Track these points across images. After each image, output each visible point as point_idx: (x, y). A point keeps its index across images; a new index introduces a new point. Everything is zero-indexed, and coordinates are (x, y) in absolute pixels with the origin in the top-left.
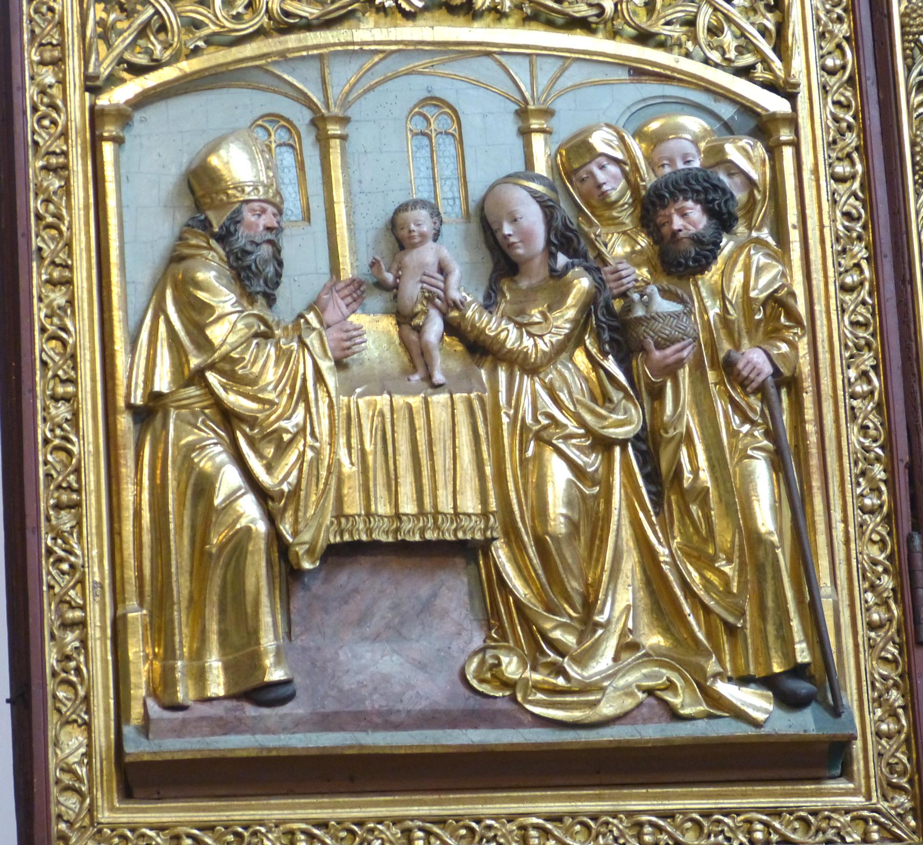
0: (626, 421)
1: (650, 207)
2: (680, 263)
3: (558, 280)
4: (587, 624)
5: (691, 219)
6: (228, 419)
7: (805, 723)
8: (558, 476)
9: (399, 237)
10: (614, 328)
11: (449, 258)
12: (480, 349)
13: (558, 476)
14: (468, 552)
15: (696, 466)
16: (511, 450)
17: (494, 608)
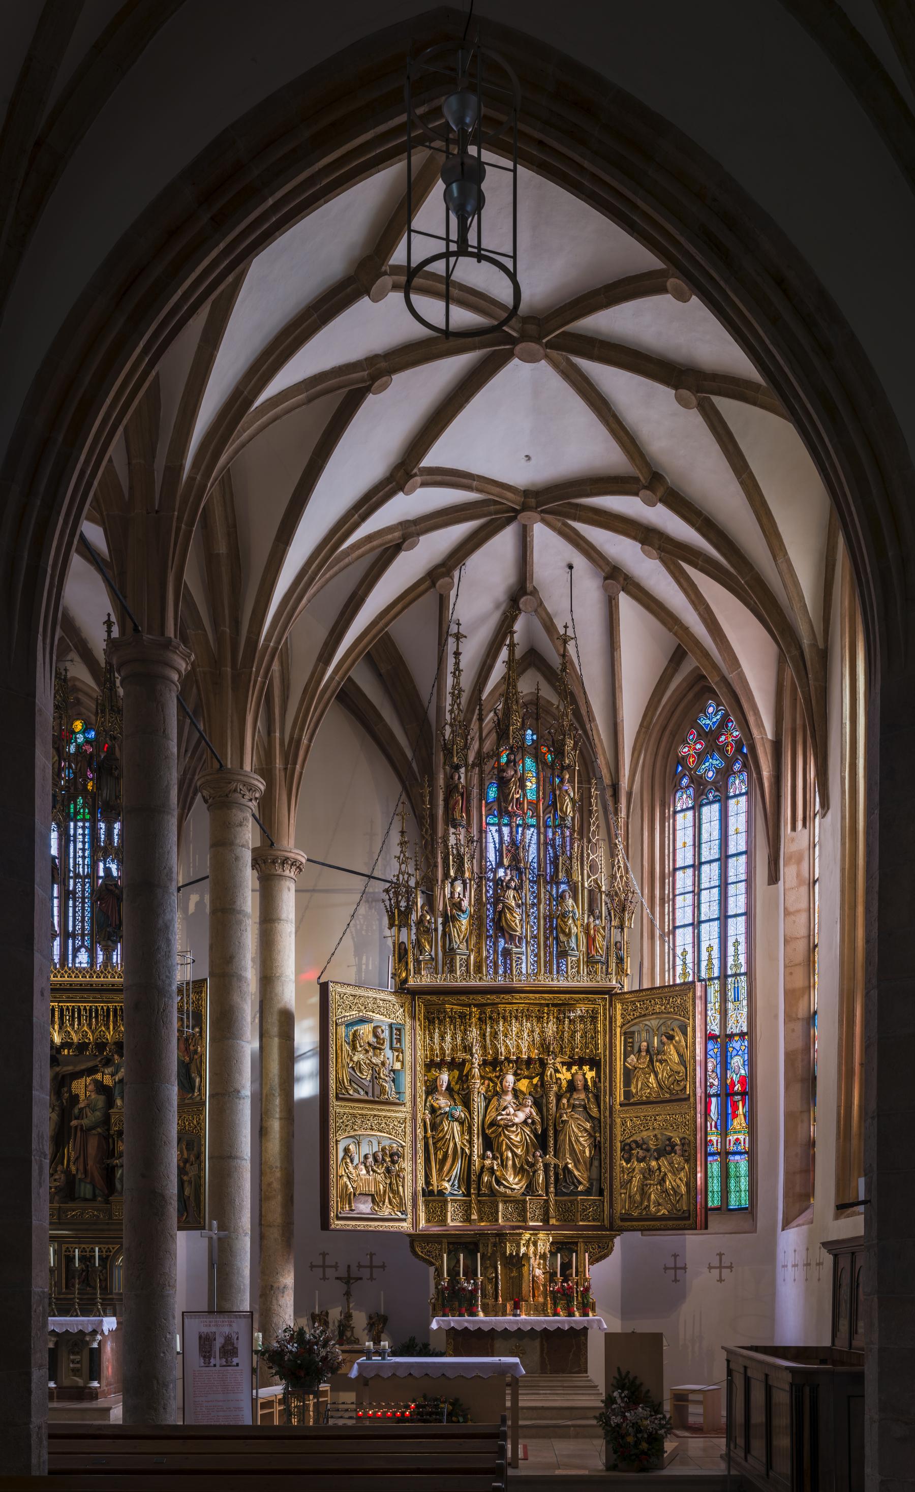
0: (388, 1181)
1: (391, 1156)
2: (393, 1162)
3: (382, 1164)
4: (383, 1204)
5: (396, 1158)
6: (348, 1177)
7: (403, 1217)
8: (381, 1187)
9: (366, 1157)
10: (388, 1170)
11: (371, 1159)
12: (374, 1171)
13: (381, 1187)
14: (372, 1195)
15: (395, 1188)
16: (376, 1183)
17: (374, 1201)
